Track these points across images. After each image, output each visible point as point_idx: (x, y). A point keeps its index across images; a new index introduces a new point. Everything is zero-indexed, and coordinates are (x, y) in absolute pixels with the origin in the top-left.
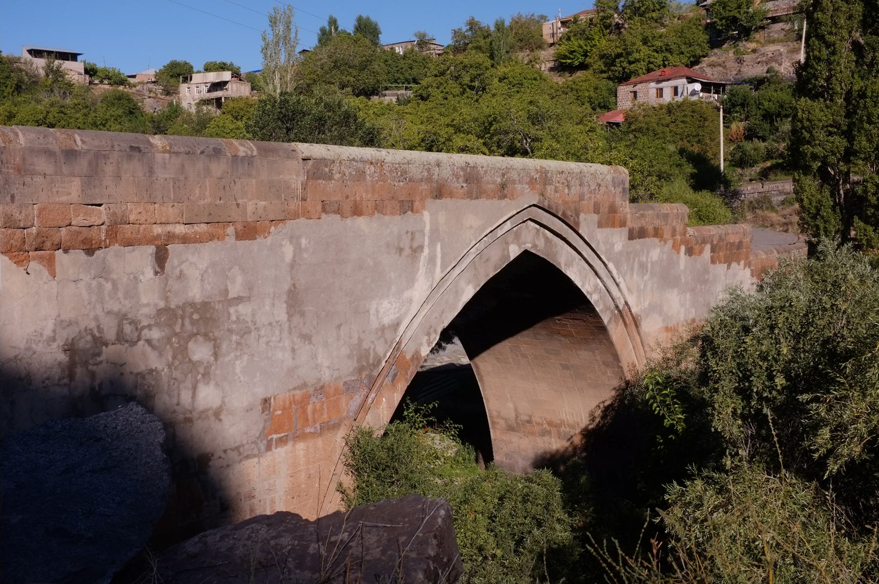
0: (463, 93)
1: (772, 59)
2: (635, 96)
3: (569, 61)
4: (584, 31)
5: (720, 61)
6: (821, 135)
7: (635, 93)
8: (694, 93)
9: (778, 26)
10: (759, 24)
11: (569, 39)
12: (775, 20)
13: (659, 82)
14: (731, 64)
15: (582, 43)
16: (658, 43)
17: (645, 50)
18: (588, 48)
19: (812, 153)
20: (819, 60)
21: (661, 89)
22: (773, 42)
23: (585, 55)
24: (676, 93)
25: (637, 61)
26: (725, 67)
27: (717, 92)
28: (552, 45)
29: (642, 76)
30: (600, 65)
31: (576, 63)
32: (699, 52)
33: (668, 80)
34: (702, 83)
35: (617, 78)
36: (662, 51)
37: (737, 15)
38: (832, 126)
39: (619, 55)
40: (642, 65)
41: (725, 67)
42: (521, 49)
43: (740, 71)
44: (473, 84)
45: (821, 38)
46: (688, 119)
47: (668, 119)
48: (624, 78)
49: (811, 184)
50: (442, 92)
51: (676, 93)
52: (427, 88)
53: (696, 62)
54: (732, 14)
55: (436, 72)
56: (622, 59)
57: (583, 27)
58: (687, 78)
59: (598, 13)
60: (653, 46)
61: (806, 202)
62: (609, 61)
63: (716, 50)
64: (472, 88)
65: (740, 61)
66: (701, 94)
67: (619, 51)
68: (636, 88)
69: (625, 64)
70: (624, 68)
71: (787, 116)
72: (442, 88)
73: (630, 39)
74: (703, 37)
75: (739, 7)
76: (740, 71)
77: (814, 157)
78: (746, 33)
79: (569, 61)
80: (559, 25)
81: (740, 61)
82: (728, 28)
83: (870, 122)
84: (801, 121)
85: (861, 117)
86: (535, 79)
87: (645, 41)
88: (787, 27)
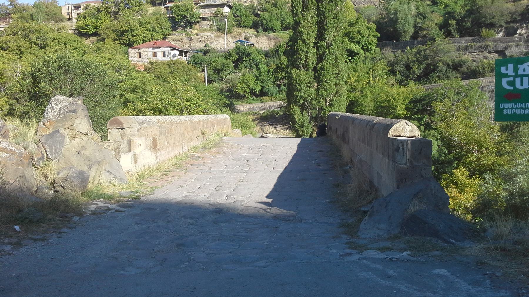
0: (31, 47)
1: (207, 40)
2: (140, 57)
3: (86, 31)
4: (94, 14)
5: (179, 38)
6: (303, 86)
7: (140, 54)
8: (174, 56)
9: (206, 22)
10: (197, 20)
11: (85, 17)
12: (204, 19)
13: (154, 48)
14: (185, 40)
15: (94, 20)
16: (148, 26)
17: (141, 30)
18: (98, 24)
19: (301, 96)
20: (303, 51)
21: (156, 53)
22: (205, 30)
23: (96, 28)
24: (164, 55)
25: (138, 35)
26: (182, 42)
27: (186, 56)
28: (69, 19)
29: (141, 45)
30: (113, 35)
31: (91, 32)
32: (166, 32)
33: (160, 48)
34: (179, 50)
35: (124, 44)
36: (150, 31)
37: (186, 14)
38: (308, 83)
39: (127, 31)
40: (140, 38)
41: (182, 42)
42: (48, 20)
43: (190, 44)
44: (38, 42)
45: (304, 42)
46: (179, 71)
47: (169, 70)
48: (130, 45)
49: (297, 109)
50: (17, 46)
51: (164, 55)
52: (6, 43)
53: (165, 38)
54: (183, 13)
55: (11, 33)
56: (128, 33)
57: (94, 11)
58: (171, 47)
59: (102, 3)
60: (145, 27)
61: (297, 120)
62: (122, 34)
63: (174, 32)
64: (36, 44)
65: (190, 40)
66: (179, 57)
67: (127, 29)
68: (140, 51)
69: (130, 37)
70: (129, 39)
71: (290, 77)
72: (16, 44)
73: (132, 23)
74: (168, 24)
75: (187, 10)
76: (190, 44)
77: (301, 97)
78: (189, 24)
79: (86, 31)
80: (73, 8)
81: (190, 40)
82: (181, 21)
83: (325, 82)
84: (296, 80)
85: (323, 79)
86: (74, 41)
87: (140, 24)
88: (211, 23)
